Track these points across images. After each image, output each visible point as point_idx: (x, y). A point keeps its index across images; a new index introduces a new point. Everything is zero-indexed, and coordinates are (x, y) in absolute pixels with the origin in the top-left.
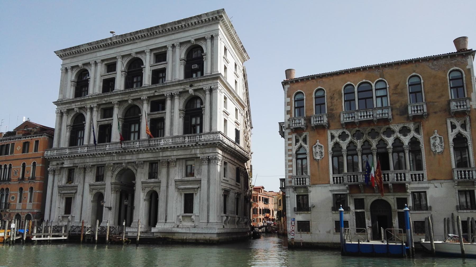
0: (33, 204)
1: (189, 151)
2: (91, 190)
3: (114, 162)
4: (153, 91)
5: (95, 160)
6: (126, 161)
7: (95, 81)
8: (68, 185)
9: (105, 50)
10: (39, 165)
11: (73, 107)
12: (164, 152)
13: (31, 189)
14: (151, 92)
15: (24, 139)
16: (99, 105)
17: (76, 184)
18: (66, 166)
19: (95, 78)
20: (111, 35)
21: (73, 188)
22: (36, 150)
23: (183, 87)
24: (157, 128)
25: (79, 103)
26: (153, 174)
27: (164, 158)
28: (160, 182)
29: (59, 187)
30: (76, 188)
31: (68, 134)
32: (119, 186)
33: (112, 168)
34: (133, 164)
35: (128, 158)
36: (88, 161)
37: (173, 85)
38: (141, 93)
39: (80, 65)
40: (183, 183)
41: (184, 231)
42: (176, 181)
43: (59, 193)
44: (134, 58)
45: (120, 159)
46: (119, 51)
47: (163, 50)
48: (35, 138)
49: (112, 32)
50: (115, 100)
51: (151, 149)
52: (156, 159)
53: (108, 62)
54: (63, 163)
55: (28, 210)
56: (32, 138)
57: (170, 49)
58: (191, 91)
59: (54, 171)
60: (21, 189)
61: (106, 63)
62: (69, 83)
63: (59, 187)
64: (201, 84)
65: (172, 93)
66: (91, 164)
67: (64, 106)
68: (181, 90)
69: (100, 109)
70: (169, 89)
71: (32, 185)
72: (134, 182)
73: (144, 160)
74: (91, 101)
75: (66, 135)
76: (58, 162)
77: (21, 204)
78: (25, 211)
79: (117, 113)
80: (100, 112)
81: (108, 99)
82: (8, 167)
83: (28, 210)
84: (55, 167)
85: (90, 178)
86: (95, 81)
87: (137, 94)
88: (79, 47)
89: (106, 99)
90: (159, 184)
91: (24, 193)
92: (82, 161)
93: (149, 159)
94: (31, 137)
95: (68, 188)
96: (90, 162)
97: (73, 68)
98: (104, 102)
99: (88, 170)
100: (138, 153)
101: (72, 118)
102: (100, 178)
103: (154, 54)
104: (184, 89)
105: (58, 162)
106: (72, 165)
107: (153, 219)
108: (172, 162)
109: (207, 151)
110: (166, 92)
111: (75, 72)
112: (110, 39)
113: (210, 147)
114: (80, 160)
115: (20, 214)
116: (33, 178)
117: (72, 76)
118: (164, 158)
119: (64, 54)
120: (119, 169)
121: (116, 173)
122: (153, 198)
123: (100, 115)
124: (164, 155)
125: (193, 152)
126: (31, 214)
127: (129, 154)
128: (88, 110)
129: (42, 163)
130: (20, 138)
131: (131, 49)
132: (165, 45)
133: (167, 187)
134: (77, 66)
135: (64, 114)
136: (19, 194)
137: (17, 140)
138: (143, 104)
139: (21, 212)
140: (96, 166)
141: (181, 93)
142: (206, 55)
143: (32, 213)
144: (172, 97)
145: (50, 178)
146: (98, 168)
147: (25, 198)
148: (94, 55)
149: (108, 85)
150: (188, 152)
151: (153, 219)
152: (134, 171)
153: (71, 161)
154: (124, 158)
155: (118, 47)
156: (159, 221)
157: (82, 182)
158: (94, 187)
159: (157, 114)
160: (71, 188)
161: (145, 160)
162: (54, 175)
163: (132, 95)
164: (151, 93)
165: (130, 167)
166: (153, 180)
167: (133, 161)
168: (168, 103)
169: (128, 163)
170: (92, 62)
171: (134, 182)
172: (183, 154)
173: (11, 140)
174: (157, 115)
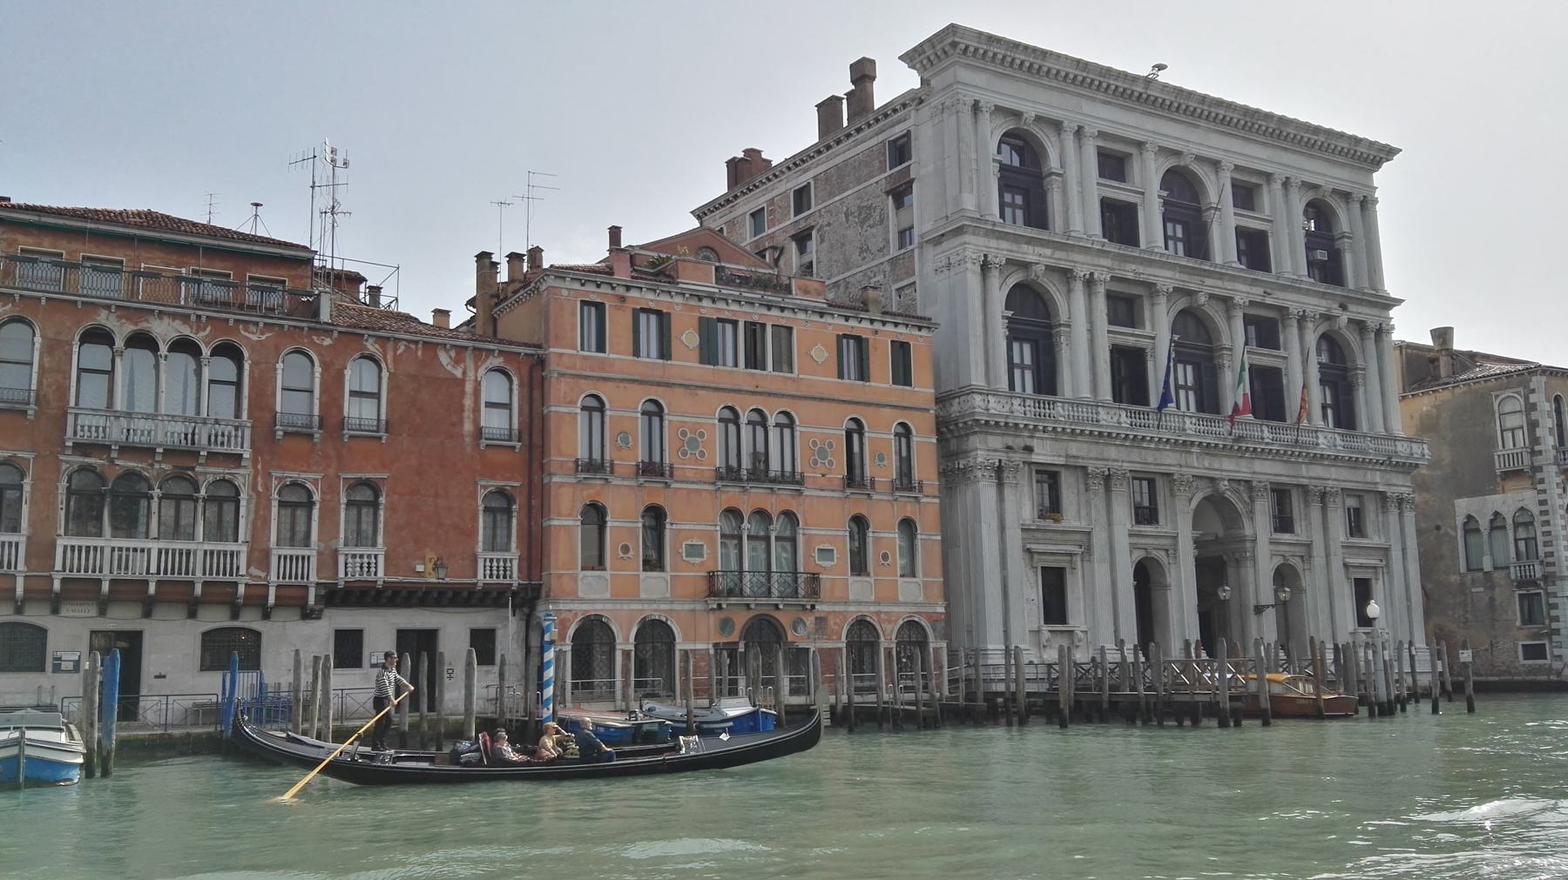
0: (926, 584)
1: (1361, 472)
3: (1195, 472)
5: (1135, 455)
11: (1030, 258)
15: (842, 322)
21: (1067, 537)
23: (1324, 303)
25: (1048, 252)
26: (1283, 523)
27: (1314, 482)
34: (1235, 485)
44: (1186, 168)
46: (1150, 127)
47: (1254, 180)
48: (889, 328)
49: (1161, 67)
52: (1294, 481)
54: (1029, 449)
55: (906, 604)
56: (877, 326)
57: (1277, 186)
70: (1294, 297)
71: (909, 510)
74: (1088, 259)
76: (1010, 441)
77: (871, 580)
78: (895, 609)
81: (1140, 269)
83: (906, 604)
84: (1003, 457)
87: (1219, 283)
91: (877, 540)
92: (1095, 451)
94: (872, 321)
95: (1049, 535)
96: (1122, 459)
97: (999, 110)
98: (1130, 276)
102: (1146, 514)
105: (1010, 441)
106: (1062, 461)
114: (1085, 446)
121: (1194, 504)
125: (1369, 477)
126: (924, 623)
128: (1079, 287)
131: (1197, 141)
132: (1269, 170)
135: (995, 273)
137: (801, 316)
138: (1229, 318)
139: (878, 613)
143: (929, 616)
147: (885, 557)
149: (1120, 222)
150: (1358, 476)
152: (1239, 506)
153: (1058, 445)
154: (1216, 466)
155: (1150, 114)
157: (1103, 519)
160: (1059, 537)
162: (1000, 485)
163: (1208, 281)
170: (1070, 126)
173: (769, 308)
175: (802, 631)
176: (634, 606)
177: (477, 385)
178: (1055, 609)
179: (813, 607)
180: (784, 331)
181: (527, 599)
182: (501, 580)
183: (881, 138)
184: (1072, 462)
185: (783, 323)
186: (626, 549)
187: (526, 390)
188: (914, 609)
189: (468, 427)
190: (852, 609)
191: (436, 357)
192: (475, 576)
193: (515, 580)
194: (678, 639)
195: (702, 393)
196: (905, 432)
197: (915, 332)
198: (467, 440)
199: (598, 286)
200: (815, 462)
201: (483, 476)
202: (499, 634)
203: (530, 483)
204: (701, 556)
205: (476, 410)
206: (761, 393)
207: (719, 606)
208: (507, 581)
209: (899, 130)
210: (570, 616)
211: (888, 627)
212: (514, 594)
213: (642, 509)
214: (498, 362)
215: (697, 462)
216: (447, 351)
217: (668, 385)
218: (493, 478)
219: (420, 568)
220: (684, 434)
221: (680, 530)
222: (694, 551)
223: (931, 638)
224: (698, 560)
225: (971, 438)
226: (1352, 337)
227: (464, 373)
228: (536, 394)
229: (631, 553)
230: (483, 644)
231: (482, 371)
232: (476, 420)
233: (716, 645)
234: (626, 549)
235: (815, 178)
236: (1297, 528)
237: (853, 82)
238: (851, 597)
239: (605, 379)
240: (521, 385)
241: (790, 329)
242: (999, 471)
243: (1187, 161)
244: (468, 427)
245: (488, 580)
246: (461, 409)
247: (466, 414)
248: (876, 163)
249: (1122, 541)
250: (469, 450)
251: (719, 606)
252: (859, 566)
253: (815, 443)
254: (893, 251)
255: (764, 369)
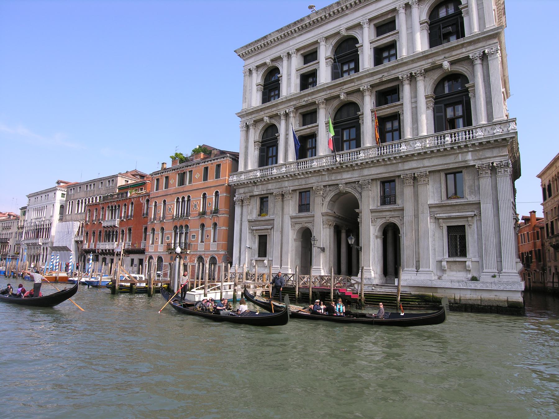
1: (453, 157)
2: (293, 225)
3: (325, 184)
4: (380, 76)
5: (296, 183)
6: (344, 181)
7: (289, 79)
8: (260, 218)
9: (301, 35)
10: (223, 195)
12: (405, 163)
13: (215, 225)
14: (375, 77)
15: (203, 164)
16: (297, 109)
17: (272, 217)
18: (257, 193)
19: (289, 75)
20: (309, 12)
21: (267, 222)
22: (218, 176)
23: (430, 61)
24: (389, 126)
26: (387, 198)
28: (402, 210)
29: (250, 221)
30: (272, 222)
31: (257, 153)
32: (331, 218)
33: (321, 192)
34: (353, 185)
35: (347, 176)
36: (286, 186)
37: (413, 61)
38: (359, 82)
39: (268, 61)
40: (444, 208)
41: (449, 285)
42: (431, 206)
43: (249, 229)
44: (344, 36)
45: (333, 178)
47: (389, 16)
48: (216, 161)
49: (311, 7)
50: (319, 98)
51: (384, 160)
52: (392, 175)
53: (305, 51)
56: (213, 162)
57: (402, 11)
58: (446, 65)
59: (242, 201)
60: (203, 226)
61: (302, 52)
62: (255, 88)
63: (250, 221)
64: (464, 50)
65: (411, 74)
66: (292, 188)
67: (250, 117)
68: (426, 66)
69: (298, 114)
70: (405, 68)
72: (357, 210)
73: (371, 177)
75: (254, 154)
77: (203, 244)
79: (324, 118)
80: (298, 118)
81: (310, 98)
82: (186, 199)
84: (244, 195)
85: (291, 207)
86: (289, 79)
87: (353, 84)
88: (265, 37)
89: (306, 99)
90: (401, 212)
92: (278, 185)
93: (380, 176)
96: (289, 186)
97: (258, 67)
98: (304, 103)
99: (287, 197)
100: (363, 168)
101: (261, 131)
102: (304, 207)
103: (374, 25)
104: (434, 63)
106: (265, 192)
107: (391, 266)
108: (421, 176)
109: (487, 156)
110: (402, 73)
111: (262, 72)
112: (309, 16)
113: (493, 148)
114: (275, 184)
115: (203, 257)
116: (216, 211)
117: (257, 78)
118: (408, 172)
119: (246, 53)
120: (333, 194)
121: (328, 199)
122: (391, 236)
123: (298, 122)
124: (406, 168)
126: (217, 258)
127: (348, 171)
128: (282, 118)
129: (226, 192)
130: (199, 164)
132: (393, 7)
133: (416, 216)
134: (265, 64)
135: (251, 127)
136: (200, 231)
139: (204, 254)
140: (298, 192)
141: (426, 71)
142: (467, 7)
143: (217, 255)
144: (412, 78)
145: (238, 210)
146: (300, 193)
147: (208, 236)
148: (285, 45)
149: (308, 79)
151: (391, 266)
152: (357, 195)
155: (319, 26)
156: (405, 269)
158: (297, 220)
159: (388, 108)
161: (375, 177)
163: (345, 87)
164: (376, 79)
165: (349, 190)
166: (388, 207)
167: (353, 180)
168: (406, 90)
169: (346, 183)
171: (357, 210)
172: (441, 163)
173: (187, 166)
174: (387, 110)
178: (263, 251)
184: (269, 192)
197: (222, 159)
217: (167, 195)
222: (168, 238)
226: (461, 69)
236: (399, 201)
238: (199, 250)
242: (242, 201)
243: (344, 33)
249: (288, 222)
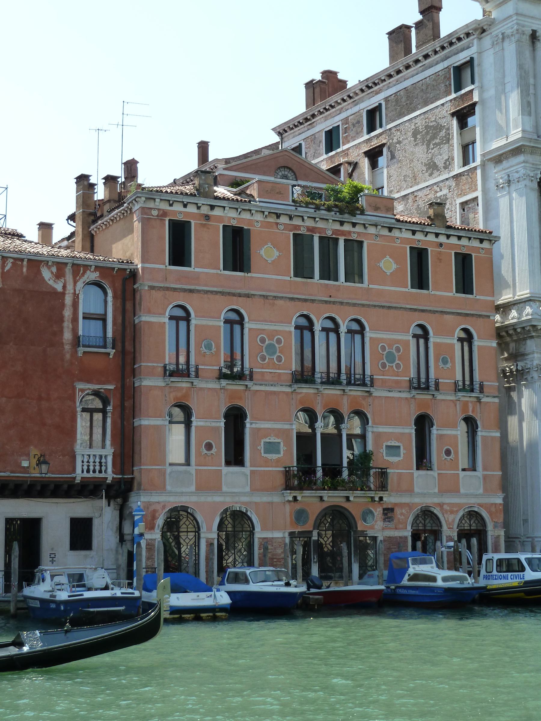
0: (485, 477)
15: (409, 235)
48: (453, 241)
55: (466, 495)
56: (442, 239)
77: (434, 473)
91: (440, 437)
94: (437, 235)
137: (372, 230)
139: (441, 505)
147: (448, 453)
175: (370, 522)
176: (218, 499)
177: (76, 297)
179: (381, 499)
180: (355, 245)
181: (120, 491)
182: (97, 475)
183: (446, 64)
185: (354, 237)
186: (209, 446)
187: (119, 302)
188: (472, 501)
189: (67, 336)
190: (417, 500)
191: (39, 272)
192: (74, 470)
193: (110, 475)
194: (258, 529)
195: (280, 302)
196: (468, 338)
198: (67, 347)
199: (185, 206)
200: (384, 365)
201: (81, 380)
202: (96, 523)
203: (123, 386)
204: (278, 452)
205: (75, 320)
206: (334, 303)
207: (295, 498)
208: (102, 475)
209: (462, 57)
210: (158, 507)
211: (451, 517)
212: (109, 487)
213: (224, 410)
214: (93, 276)
215: (275, 367)
216: (49, 267)
217: (248, 296)
218: (89, 381)
219: (25, 464)
220: (263, 340)
221: (259, 429)
222: (272, 448)
223: (490, 527)
224: (274, 456)
225: (529, 342)
227: (64, 287)
228: (129, 305)
229: (214, 450)
230: (81, 535)
231: (80, 284)
232: (75, 330)
233: (292, 534)
234: (209, 446)
235: (386, 99)
237: (422, 13)
238: (416, 490)
239: (191, 291)
240: (115, 297)
241: (361, 243)
244: (67, 336)
245: (85, 475)
246: (61, 320)
247: (65, 324)
248: (442, 87)
250: (68, 356)
251: (295, 498)
252: (423, 459)
253: (383, 348)
254: (457, 169)
255: (336, 279)
